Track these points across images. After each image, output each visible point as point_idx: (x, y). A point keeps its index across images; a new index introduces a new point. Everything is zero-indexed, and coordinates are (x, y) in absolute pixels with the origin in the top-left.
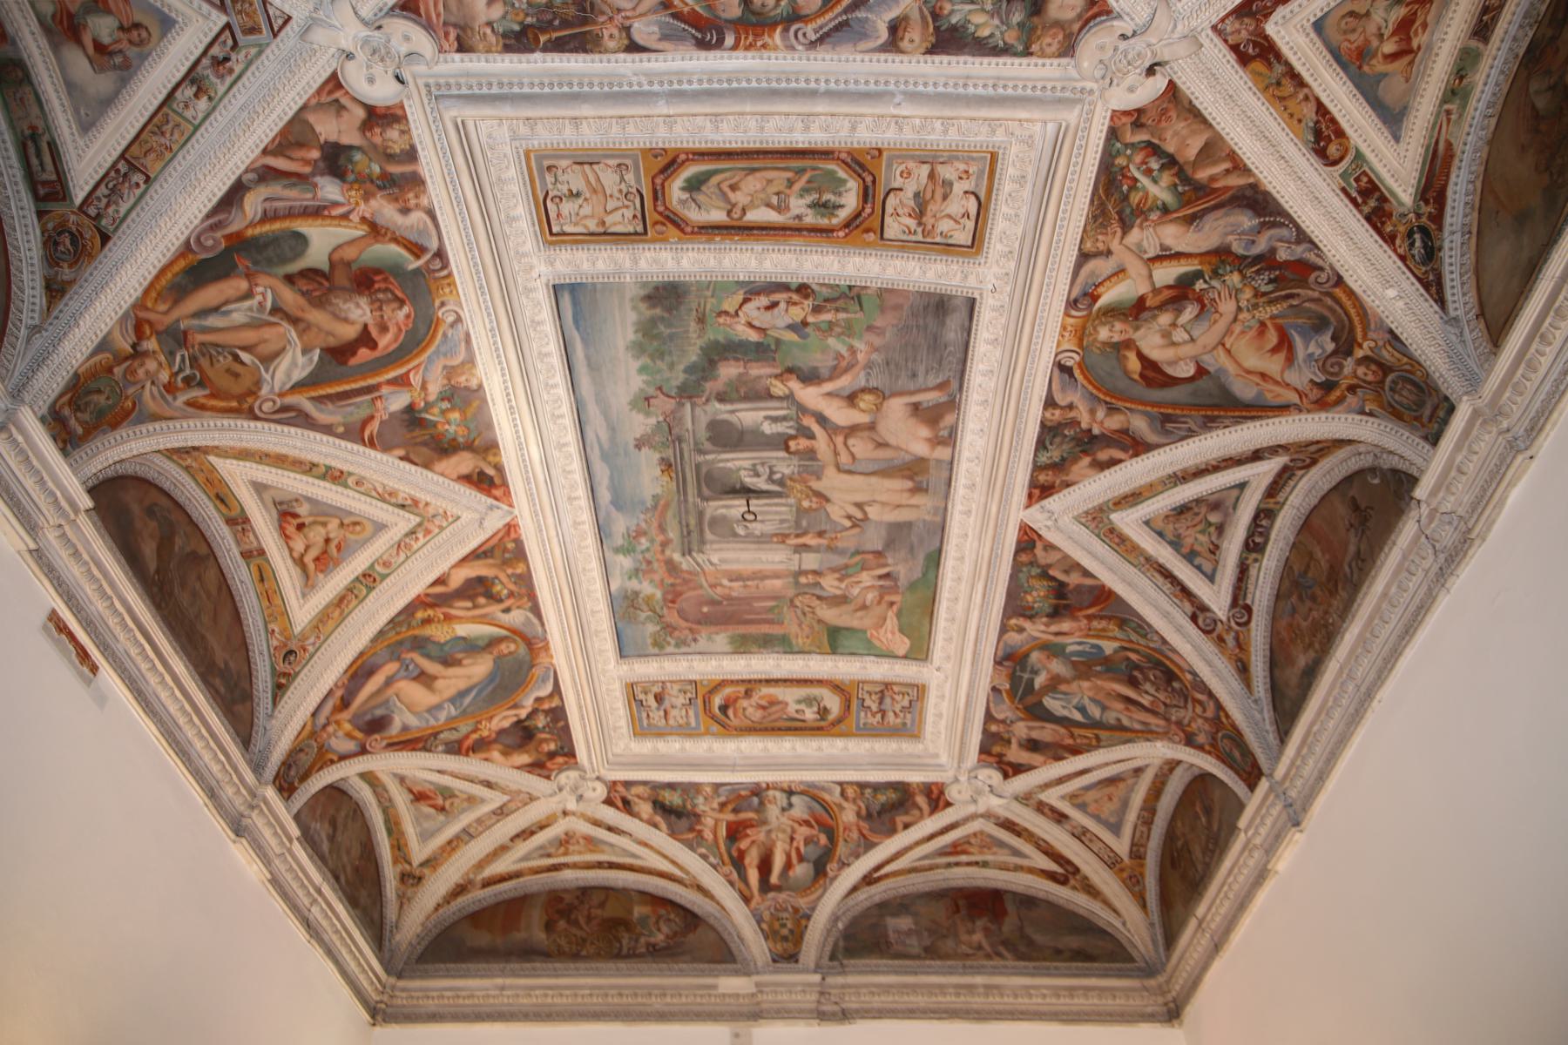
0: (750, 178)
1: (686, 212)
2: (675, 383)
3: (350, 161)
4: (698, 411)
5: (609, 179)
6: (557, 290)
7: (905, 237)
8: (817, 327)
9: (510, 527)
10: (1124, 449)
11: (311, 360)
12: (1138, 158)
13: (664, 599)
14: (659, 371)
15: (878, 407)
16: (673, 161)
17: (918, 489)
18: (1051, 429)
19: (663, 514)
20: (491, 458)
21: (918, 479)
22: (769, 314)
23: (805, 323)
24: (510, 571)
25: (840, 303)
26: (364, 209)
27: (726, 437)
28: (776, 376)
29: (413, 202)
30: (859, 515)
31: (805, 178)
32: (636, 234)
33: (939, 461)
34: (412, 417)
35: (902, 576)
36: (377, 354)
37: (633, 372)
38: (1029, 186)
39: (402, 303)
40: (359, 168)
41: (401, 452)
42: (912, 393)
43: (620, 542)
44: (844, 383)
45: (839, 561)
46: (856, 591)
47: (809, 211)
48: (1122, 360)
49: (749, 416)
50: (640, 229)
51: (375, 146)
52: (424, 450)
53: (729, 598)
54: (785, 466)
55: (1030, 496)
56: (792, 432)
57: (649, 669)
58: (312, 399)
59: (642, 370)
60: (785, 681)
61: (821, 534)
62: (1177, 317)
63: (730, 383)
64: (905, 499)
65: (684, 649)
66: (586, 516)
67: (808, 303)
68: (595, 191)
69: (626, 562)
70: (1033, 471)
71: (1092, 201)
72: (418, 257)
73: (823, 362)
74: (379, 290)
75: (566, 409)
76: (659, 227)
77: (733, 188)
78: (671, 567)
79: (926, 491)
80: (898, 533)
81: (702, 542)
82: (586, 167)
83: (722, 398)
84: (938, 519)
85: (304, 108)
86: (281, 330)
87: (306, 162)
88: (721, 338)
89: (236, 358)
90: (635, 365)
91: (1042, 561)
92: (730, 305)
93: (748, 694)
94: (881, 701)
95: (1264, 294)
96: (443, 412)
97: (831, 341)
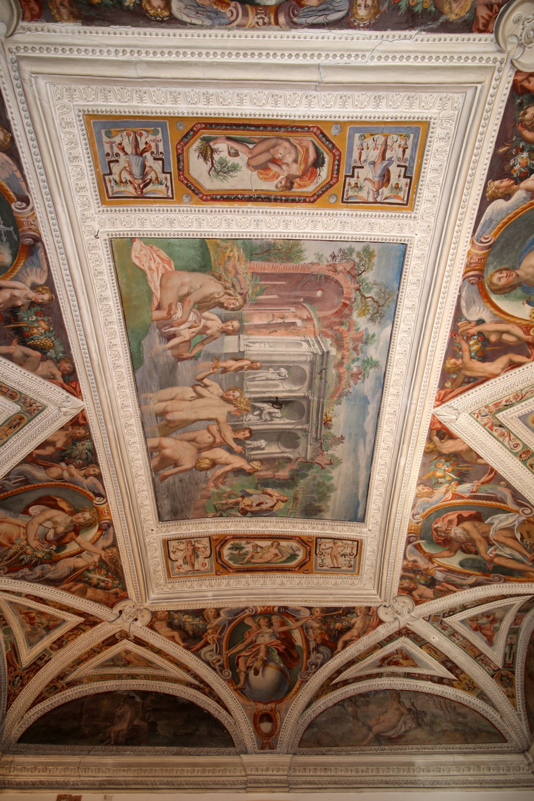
0: (269, 559)
2: (312, 470)
3: (426, 581)
4: (303, 455)
5: (328, 561)
6: (363, 520)
8: (236, 496)
9: (441, 400)
10: (39, 456)
11: (492, 520)
14: (321, 477)
16: (300, 567)
17: (162, 414)
18: (91, 462)
19: (337, 389)
21: (165, 422)
22: (261, 501)
23: (243, 497)
24: (459, 362)
25: (225, 507)
26: (431, 566)
28: (257, 471)
30: (199, 388)
33: (154, 436)
34: (462, 477)
35: (157, 340)
36: (460, 512)
37: (335, 478)
39: (436, 529)
40: (424, 579)
41: (480, 461)
44: (219, 471)
45: (210, 347)
46: (192, 317)
47: (244, 546)
49: (274, 450)
50: (319, 540)
51: (414, 583)
52: (466, 458)
53: (296, 304)
54: (251, 418)
55: (85, 418)
56: (248, 442)
58: (505, 503)
59: (331, 478)
60: (250, 199)
61: (225, 370)
62: (55, 532)
63: (283, 467)
64: (170, 406)
65: (346, 246)
67: (242, 506)
69: (373, 352)
72: (419, 544)
73: (232, 480)
76: (310, 540)
77: (276, 555)
79: (156, 415)
81: (312, 363)
82: (336, 566)
83: (289, 460)
84: (143, 396)
85: (434, 599)
86: (495, 537)
87: (443, 586)
88: (286, 490)
89: (522, 538)
90: (333, 481)
91: (50, 363)
92: (281, 505)
93: (290, 182)
94: (144, 174)
95: (22, 554)
96: (444, 477)
97: (228, 490)
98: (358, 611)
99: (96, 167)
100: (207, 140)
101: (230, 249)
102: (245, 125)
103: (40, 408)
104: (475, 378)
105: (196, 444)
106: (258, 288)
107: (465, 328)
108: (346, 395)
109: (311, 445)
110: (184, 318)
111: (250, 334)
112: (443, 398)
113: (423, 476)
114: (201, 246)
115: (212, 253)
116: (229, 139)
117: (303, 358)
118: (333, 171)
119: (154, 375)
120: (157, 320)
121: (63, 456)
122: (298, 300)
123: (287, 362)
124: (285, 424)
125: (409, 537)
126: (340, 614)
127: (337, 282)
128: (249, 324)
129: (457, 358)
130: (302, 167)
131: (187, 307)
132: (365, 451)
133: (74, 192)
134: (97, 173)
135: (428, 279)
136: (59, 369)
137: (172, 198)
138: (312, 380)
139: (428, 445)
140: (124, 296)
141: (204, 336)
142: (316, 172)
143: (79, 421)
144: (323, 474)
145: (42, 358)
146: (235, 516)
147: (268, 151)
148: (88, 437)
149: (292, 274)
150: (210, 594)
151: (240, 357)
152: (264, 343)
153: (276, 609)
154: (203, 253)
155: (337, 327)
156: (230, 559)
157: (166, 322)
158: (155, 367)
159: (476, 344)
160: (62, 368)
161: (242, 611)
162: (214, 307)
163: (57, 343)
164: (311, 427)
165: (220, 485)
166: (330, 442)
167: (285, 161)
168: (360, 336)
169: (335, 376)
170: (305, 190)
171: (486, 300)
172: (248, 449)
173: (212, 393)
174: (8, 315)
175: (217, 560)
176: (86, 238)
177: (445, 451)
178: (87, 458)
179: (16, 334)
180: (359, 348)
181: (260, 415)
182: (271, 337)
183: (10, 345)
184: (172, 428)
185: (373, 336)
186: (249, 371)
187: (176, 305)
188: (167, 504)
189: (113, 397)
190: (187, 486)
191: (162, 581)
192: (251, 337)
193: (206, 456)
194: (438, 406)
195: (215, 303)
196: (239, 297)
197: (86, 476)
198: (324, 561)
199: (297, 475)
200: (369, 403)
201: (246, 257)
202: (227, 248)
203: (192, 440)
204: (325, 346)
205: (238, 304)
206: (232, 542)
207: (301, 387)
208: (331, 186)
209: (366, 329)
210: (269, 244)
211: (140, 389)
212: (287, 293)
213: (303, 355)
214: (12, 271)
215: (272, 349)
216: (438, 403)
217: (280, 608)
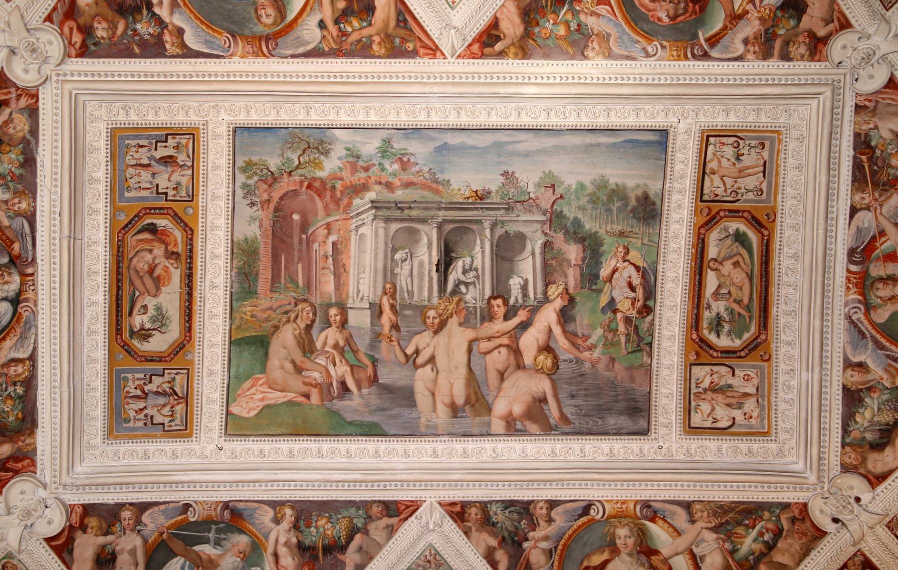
0: (744, 275)
1: (718, 230)
2: (566, 211)
3: (790, 17)
4: (539, 226)
5: (751, 182)
9: (434, 51)
12: (770, 526)
13: (315, 179)
15: (540, 371)
16: (762, 226)
17: (455, 410)
19: (425, 187)
20: (513, 50)
21: (467, 408)
22: (625, 285)
23: (615, 311)
25: (633, 337)
26: (754, 15)
27: (506, 249)
28: (566, 290)
29: (752, 49)
30: (419, 361)
33: (489, 424)
35: (347, 403)
37: (580, 178)
38: (746, 459)
39: (673, 18)
40: (784, 21)
42: (556, 396)
43: (396, 146)
44: (561, 342)
45: (363, 344)
46: (322, 361)
47: (714, 314)
48: (601, 550)
49: (527, 267)
50: (706, 197)
51: (797, 36)
55: (453, 504)
56: (512, 301)
57: (216, 158)
59: (582, 186)
60: (190, 294)
61: (395, 327)
66: (436, 120)
67: (633, 314)
68: (740, 171)
69: (370, 147)
70: (480, 503)
71: (734, 502)
72: (707, 40)
74: (687, 6)
75: (554, 121)
76: (706, 211)
77: (736, 264)
78: (359, 189)
79: (455, 416)
80: (406, 396)
81: (388, 220)
82: (762, 169)
83: (547, 246)
88: (605, 248)
91: (372, 527)
92: (634, 256)
93: (172, 255)
94: (164, 394)
96: (567, 24)
97: (600, 331)
99: (155, 436)
100: (132, 334)
101: (243, 315)
102: (117, 300)
103: (433, 552)
104: (399, 13)
105: (509, 370)
106: (289, 285)
107: (331, 42)
108: (435, 174)
109: (518, 216)
110: (322, 370)
111: (347, 295)
112: (431, 49)
113: (567, 53)
114: (239, 345)
115: (247, 334)
116: (130, 314)
117: (381, 232)
118: (161, 214)
119: (394, 412)
120: (322, 400)
121: (514, 543)
122: (304, 241)
123: (386, 251)
124: (483, 252)
125: (694, 56)
126: (870, 159)
127: (282, 198)
128: (333, 296)
129: (372, 42)
130: (156, 244)
131: (308, 365)
132: (527, 141)
133: (177, 461)
134: (162, 437)
135: (269, 98)
136: (380, 519)
137: (188, 369)
138: (411, 220)
139: (511, 55)
140: (291, 432)
141: (346, 349)
142: (162, 230)
143: (458, 512)
144: (573, 197)
145: (363, 534)
146: (652, 324)
147: (141, 278)
148: (484, 506)
149: (273, 248)
150: (804, 374)
151: (377, 308)
152: (359, 279)
153: (854, 268)
154: (247, 344)
155: (338, 194)
157: (325, 390)
158: (384, 410)
159: (350, 24)
160: (378, 515)
161: (856, 326)
162: (311, 335)
163: (345, 513)
164: (488, 218)
165: (588, 343)
166: (513, 190)
167: (151, 261)
168: (348, 165)
169: (405, 191)
170: (179, 240)
171: (294, 25)
172: (524, 301)
173: (428, 345)
174: (308, 555)
175: (740, 357)
176: (223, 459)
177: (520, 30)
178: (519, 513)
179: (331, 553)
180: (365, 165)
181: (467, 285)
182: (352, 271)
183: (345, 563)
184: (477, 400)
185: (348, 149)
186: (398, 297)
187: (306, 377)
188: (624, 421)
189: (417, 465)
190: (586, 389)
191: (773, 446)
192: (351, 294)
193: (532, 359)
194: (443, 54)
195: (306, 334)
196: (300, 307)
197: (550, 520)
198: (751, 188)
199: (575, 233)
200: (446, 144)
201: (252, 298)
202: (242, 319)
203: (502, 376)
204: (364, 205)
205: (309, 309)
206: (706, 332)
207: (423, 233)
208: (176, 214)
209: (340, 158)
210: (239, 274)
211: (412, 432)
212: (296, 253)
213: (376, 232)
214: (258, 538)
215: (367, 269)
216: (438, 54)
217: (851, 261)
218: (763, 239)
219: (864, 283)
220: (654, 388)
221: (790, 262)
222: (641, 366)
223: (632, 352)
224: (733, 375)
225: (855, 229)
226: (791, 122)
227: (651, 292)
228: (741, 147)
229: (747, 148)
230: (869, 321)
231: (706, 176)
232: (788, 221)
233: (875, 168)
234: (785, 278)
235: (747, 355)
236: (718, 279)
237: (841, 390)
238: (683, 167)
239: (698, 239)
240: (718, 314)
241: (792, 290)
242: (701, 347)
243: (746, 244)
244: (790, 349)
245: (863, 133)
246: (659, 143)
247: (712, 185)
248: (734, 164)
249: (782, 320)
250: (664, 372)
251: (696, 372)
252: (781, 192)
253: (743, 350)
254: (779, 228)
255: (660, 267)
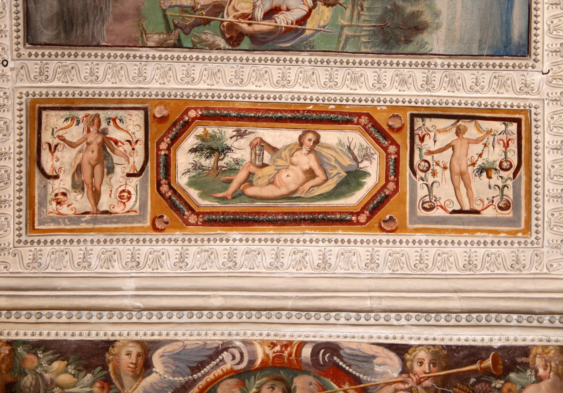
0: (293, 187)
1: (365, 144)
5: (444, 191)
6: (524, 49)
7: (120, 113)
16: (373, 212)
31: (233, 187)
32: (423, 116)
47: (229, 143)
50: (418, 122)
67: (229, 17)
68: (462, 174)
76: (397, 125)
77: (310, 174)
82: (467, 208)
98: (539, 362)
126: (486, 372)
146: (213, 47)
150: (132, 283)
153: (307, 352)
156: (192, 184)
175: (159, 185)
191: (10, 238)
198: (436, 191)
217: (317, 347)
218: (352, 214)
219: (282, 368)
220: (106, 52)
221: (316, 257)
222: (143, 32)
223: (165, 16)
224: (129, 175)
225: (371, 353)
226: (545, 250)
227: (263, 43)
228: (502, 173)
229: (500, 183)
230: (220, 377)
231: (453, 121)
232: (383, 251)
233: (473, 380)
234: (288, 249)
235: (163, 195)
236: (286, 148)
237: (105, 338)
238: (469, 84)
239: (350, 114)
240: (229, 149)
241: (269, 260)
242: (174, 124)
243: (344, 188)
244: (173, 260)
245: (530, 360)
246: (508, 41)
247: (439, 131)
248: (473, 164)
249: (220, 248)
250: (132, 67)
251: (134, 118)
252: (430, 238)
253: (171, 188)
254: (371, 238)
255: (305, 56)
